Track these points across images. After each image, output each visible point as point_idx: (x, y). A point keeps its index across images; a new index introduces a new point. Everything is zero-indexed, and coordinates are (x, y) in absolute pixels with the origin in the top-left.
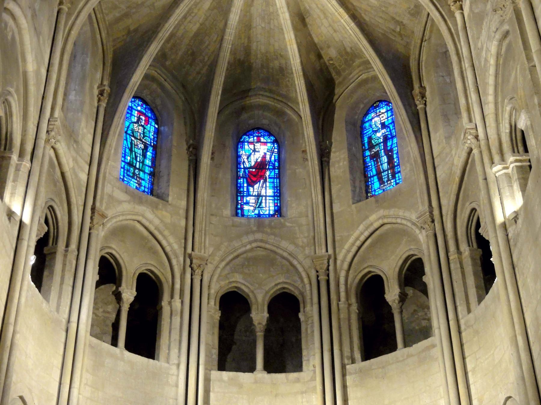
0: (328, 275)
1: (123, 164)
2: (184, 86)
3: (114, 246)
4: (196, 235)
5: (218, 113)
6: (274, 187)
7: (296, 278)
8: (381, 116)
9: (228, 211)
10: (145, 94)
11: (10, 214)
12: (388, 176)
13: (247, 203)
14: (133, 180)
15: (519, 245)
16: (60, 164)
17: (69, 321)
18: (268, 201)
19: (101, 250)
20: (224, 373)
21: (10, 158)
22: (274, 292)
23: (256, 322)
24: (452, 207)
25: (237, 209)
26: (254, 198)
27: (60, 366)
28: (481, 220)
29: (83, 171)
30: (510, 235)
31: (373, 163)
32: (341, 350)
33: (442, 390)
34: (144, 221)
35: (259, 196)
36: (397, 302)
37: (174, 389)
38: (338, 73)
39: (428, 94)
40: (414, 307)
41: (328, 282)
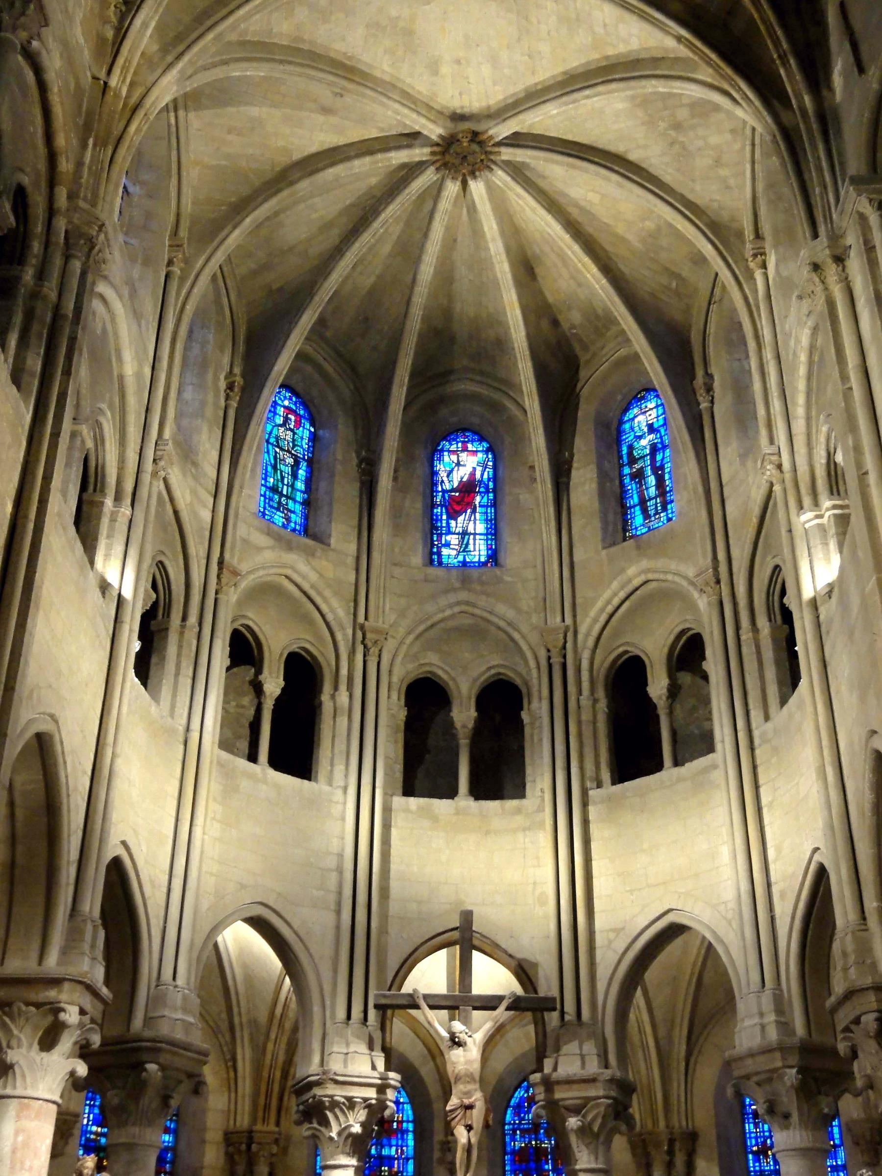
0: (564, 657)
1: (263, 489)
2: (353, 369)
3: (250, 615)
4: (371, 596)
5: (405, 409)
6: (486, 520)
7: (518, 659)
8: (648, 414)
9: (417, 559)
11: (104, 587)
12: (656, 507)
13: (448, 545)
14: (278, 513)
15: (832, 634)
16: (172, 500)
17: (188, 729)
18: (477, 542)
19: (233, 621)
20: (412, 799)
21: (102, 503)
22: (486, 680)
23: (458, 724)
25: (432, 553)
26: (457, 536)
27: (176, 794)
28: (787, 585)
29: (205, 506)
30: (822, 617)
31: (634, 486)
32: (582, 768)
33: (725, 831)
35: (464, 533)
36: (664, 698)
37: (339, 822)
38: (585, 348)
39: (717, 385)
40: (692, 701)
41: (564, 666)
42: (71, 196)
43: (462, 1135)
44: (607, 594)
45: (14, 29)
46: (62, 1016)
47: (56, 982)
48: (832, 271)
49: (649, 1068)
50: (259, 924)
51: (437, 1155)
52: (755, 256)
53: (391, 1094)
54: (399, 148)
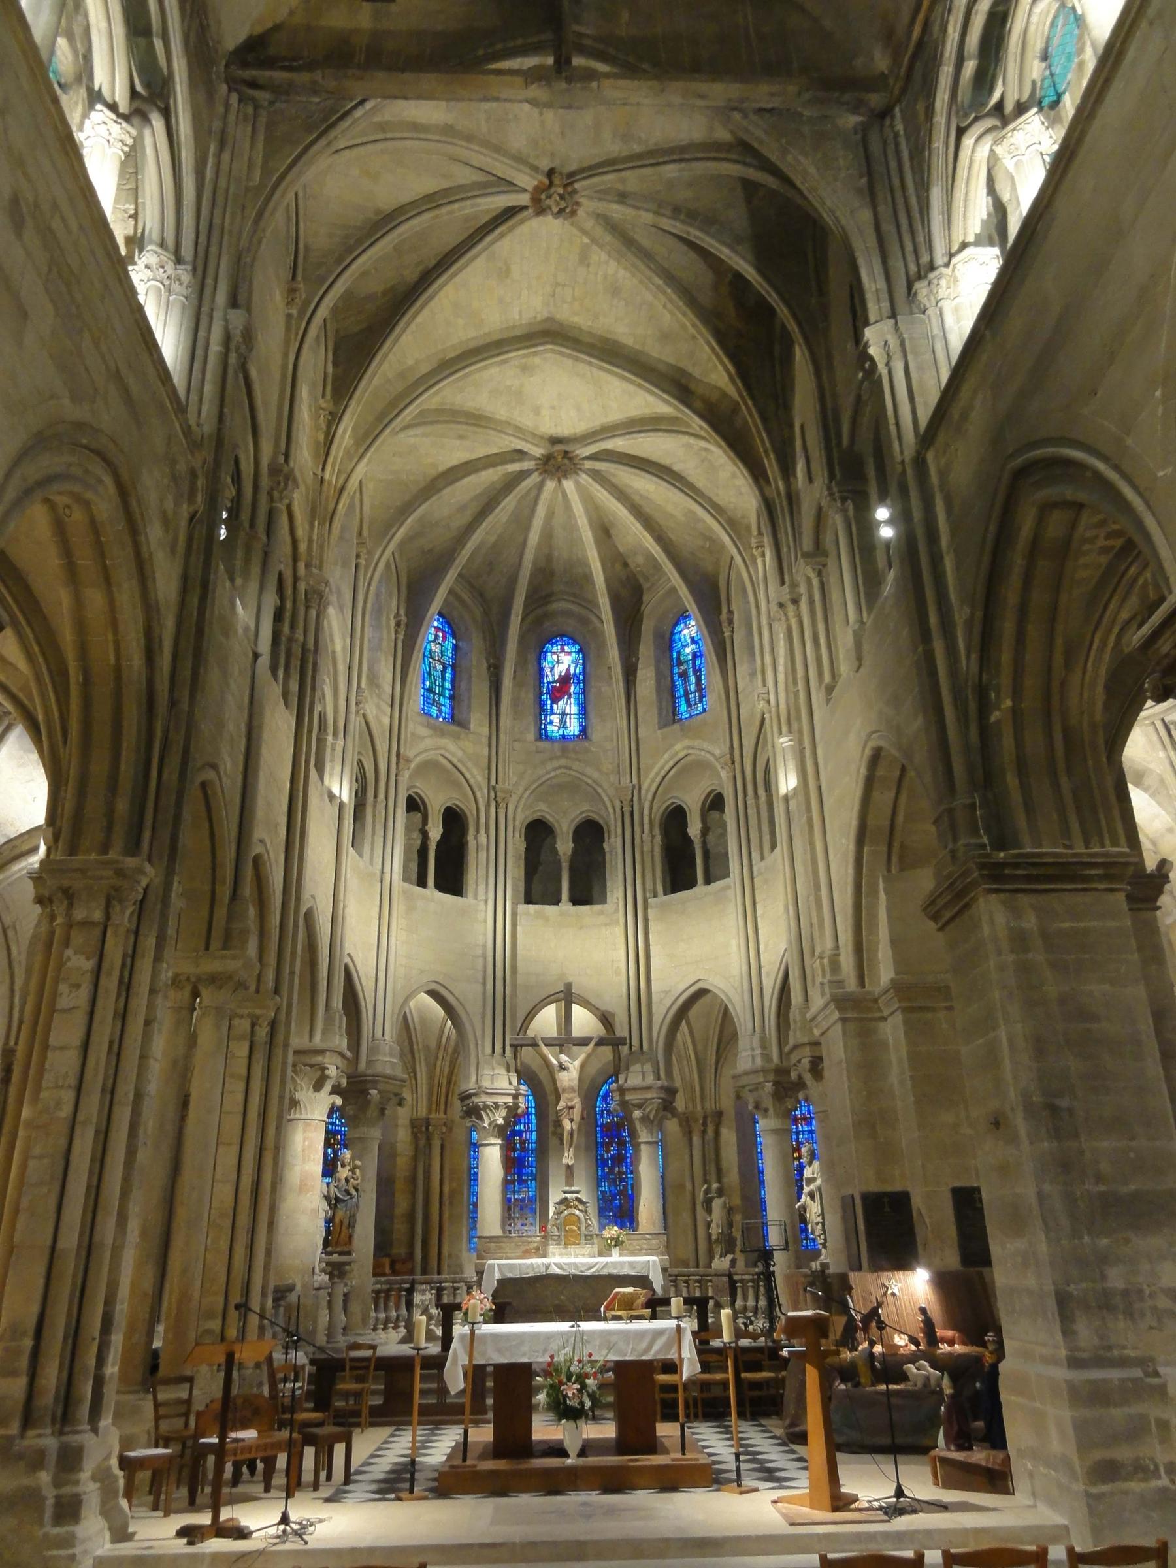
2: (481, 595)
9: (531, 736)
10: (444, 612)
11: (331, 797)
13: (551, 723)
24: (752, 750)
25: (541, 729)
34: (447, 755)
38: (647, 579)
42: (308, 566)
43: (567, 1125)
44: (662, 761)
45: (281, 499)
46: (327, 1072)
47: (322, 1052)
48: (791, 609)
49: (691, 1071)
50: (433, 994)
51: (551, 1129)
52: (757, 547)
53: (521, 1099)
54: (513, 461)
